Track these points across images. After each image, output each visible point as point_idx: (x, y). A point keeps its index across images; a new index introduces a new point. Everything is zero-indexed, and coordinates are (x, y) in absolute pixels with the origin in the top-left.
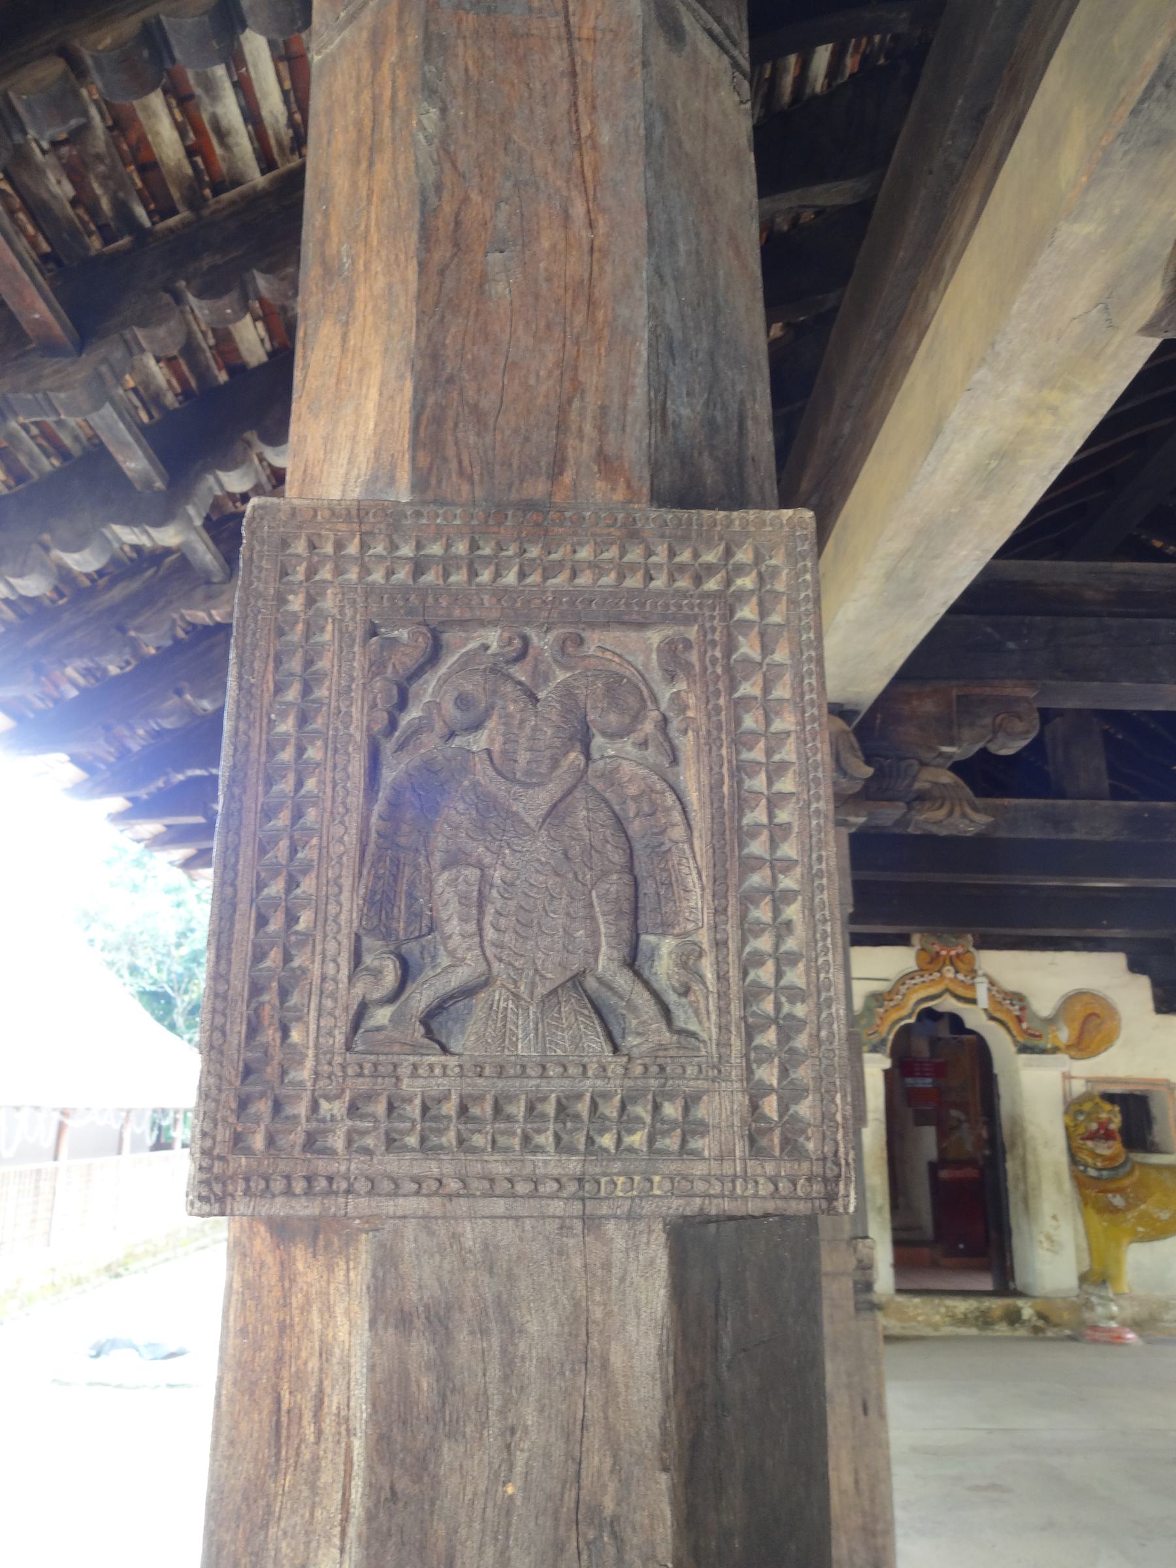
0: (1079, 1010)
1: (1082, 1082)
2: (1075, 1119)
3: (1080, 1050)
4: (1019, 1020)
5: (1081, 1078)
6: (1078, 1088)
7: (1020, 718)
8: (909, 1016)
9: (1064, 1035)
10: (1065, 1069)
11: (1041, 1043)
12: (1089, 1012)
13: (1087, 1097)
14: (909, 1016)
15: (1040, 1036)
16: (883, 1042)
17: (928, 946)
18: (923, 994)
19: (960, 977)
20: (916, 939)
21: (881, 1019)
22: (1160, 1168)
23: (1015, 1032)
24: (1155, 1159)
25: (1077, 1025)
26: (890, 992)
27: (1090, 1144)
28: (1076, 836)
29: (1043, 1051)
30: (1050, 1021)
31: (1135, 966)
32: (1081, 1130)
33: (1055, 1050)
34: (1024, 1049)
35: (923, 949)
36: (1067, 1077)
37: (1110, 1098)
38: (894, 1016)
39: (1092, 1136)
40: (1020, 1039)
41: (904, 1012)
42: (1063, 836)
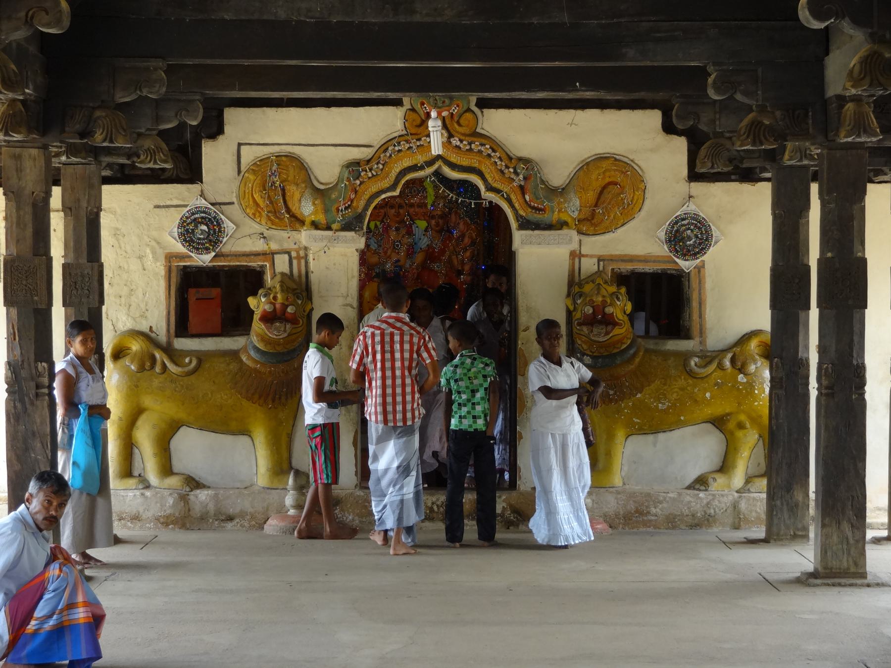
0: (596, 180)
1: (595, 260)
2: (575, 303)
3: (592, 225)
4: (522, 189)
5: (592, 256)
6: (589, 266)
7: (47, 14)
8: (393, 187)
9: (573, 207)
10: (574, 246)
11: (545, 217)
12: (607, 180)
13: (591, 278)
14: (393, 187)
15: (543, 210)
16: (360, 218)
17: (418, 107)
18: (407, 163)
19: (455, 141)
20: (406, 101)
21: (356, 192)
22: (667, 355)
23: (516, 205)
24: (673, 345)
25: (591, 196)
26: (369, 161)
27: (585, 329)
28: (417, 18)
29: (549, 227)
30: (559, 192)
31: (668, 128)
32: (578, 315)
33: (561, 225)
34: (526, 225)
35: (413, 110)
36: (575, 255)
37: (622, 279)
38: (374, 189)
39: (591, 321)
40: (522, 213)
41: (386, 184)
42: (402, 19)
